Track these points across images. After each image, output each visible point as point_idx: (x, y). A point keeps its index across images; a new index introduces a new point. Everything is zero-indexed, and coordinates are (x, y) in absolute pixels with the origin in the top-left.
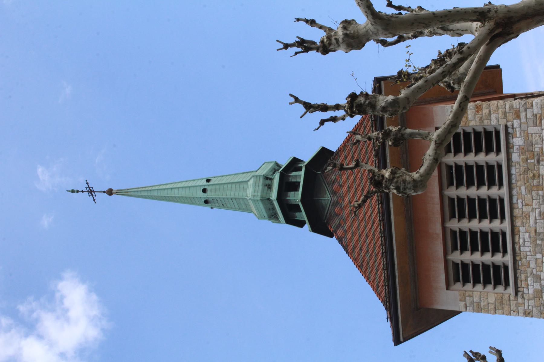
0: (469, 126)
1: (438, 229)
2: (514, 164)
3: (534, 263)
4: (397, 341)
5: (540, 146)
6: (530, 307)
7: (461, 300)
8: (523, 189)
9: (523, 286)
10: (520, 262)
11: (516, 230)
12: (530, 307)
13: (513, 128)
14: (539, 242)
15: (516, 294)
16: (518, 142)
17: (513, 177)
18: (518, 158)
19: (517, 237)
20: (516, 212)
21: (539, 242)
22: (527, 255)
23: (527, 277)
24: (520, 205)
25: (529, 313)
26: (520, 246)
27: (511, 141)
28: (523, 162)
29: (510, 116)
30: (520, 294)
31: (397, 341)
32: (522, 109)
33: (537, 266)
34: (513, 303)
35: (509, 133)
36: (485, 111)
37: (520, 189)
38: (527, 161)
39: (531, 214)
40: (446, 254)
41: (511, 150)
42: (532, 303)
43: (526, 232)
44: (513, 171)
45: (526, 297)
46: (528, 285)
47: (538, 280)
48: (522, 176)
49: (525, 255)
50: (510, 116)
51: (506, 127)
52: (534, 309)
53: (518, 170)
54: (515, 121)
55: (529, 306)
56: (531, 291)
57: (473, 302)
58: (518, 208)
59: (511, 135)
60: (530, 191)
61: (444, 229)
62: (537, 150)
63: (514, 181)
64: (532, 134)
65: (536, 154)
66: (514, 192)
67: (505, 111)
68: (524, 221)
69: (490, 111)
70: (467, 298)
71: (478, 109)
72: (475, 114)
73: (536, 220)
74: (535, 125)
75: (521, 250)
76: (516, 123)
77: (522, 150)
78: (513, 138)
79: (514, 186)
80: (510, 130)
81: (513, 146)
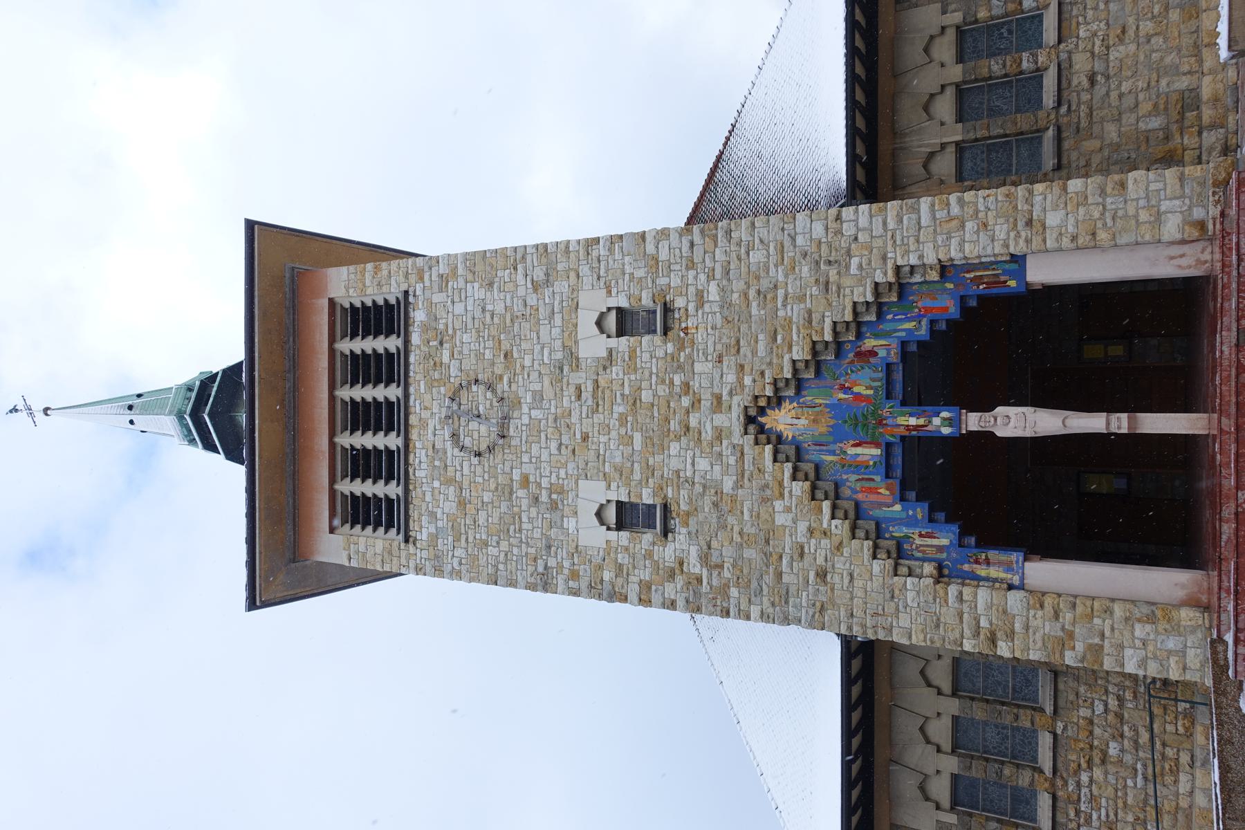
0: (366, 295)
1: (322, 443)
2: (413, 348)
3: (430, 493)
4: (252, 604)
5: (444, 321)
6: (423, 560)
7: (344, 549)
8: (422, 383)
9: (416, 529)
10: (414, 492)
11: (411, 445)
12: (423, 560)
13: (414, 296)
14: (437, 463)
15: (407, 541)
16: (418, 316)
17: (411, 367)
18: (419, 339)
19: (411, 456)
20: (413, 420)
21: (437, 463)
22: (423, 483)
23: (421, 515)
24: (418, 407)
25: (421, 569)
26: (415, 469)
27: (412, 314)
28: (424, 345)
29: (413, 279)
30: (411, 540)
31: (252, 604)
32: (426, 268)
33: (433, 499)
34: (403, 554)
35: (410, 303)
36: (385, 273)
37: (419, 386)
38: (429, 343)
39: (430, 421)
40: (332, 481)
41: (411, 328)
42: (425, 554)
43: (423, 448)
44: (412, 359)
45: (418, 545)
46: (421, 527)
47: (434, 520)
48: (422, 365)
49: (420, 482)
50: (413, 279)
51: (406, 293)
52: (427, 562)
53: (417, 358)
54: (417, 285)
55: (421, 558)
56: (424, 537)
57: (357, 552)
58: (415, 413)
59: (412, 307)
60: (430, 387)
61: (332, 445)
62: (441, 327)
63: (411, 374)
64: (436, 304)
65: (439, 331)
66: (412, 390)
67: (407, 272)
68: (422, 432)
69: (390, 272)
70: (352, 546)
71: (377, 269)
72: (374, 277)
73: (435, 430)
74: (441, 291)
75: (417, 475)
76: (419, 287)
77: (425, 328)
78: (414, 310)
79: (411, 380)
80: (411, 299)
81: (414, 322)
